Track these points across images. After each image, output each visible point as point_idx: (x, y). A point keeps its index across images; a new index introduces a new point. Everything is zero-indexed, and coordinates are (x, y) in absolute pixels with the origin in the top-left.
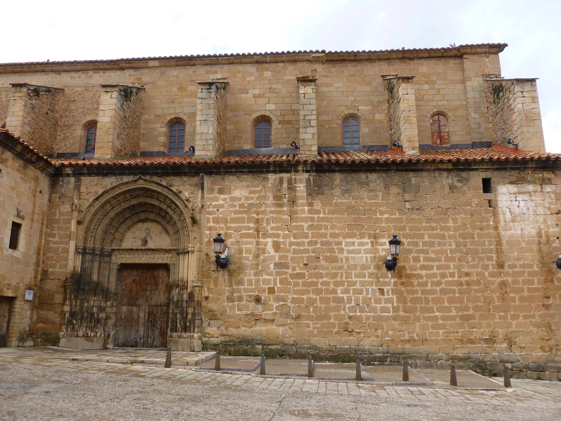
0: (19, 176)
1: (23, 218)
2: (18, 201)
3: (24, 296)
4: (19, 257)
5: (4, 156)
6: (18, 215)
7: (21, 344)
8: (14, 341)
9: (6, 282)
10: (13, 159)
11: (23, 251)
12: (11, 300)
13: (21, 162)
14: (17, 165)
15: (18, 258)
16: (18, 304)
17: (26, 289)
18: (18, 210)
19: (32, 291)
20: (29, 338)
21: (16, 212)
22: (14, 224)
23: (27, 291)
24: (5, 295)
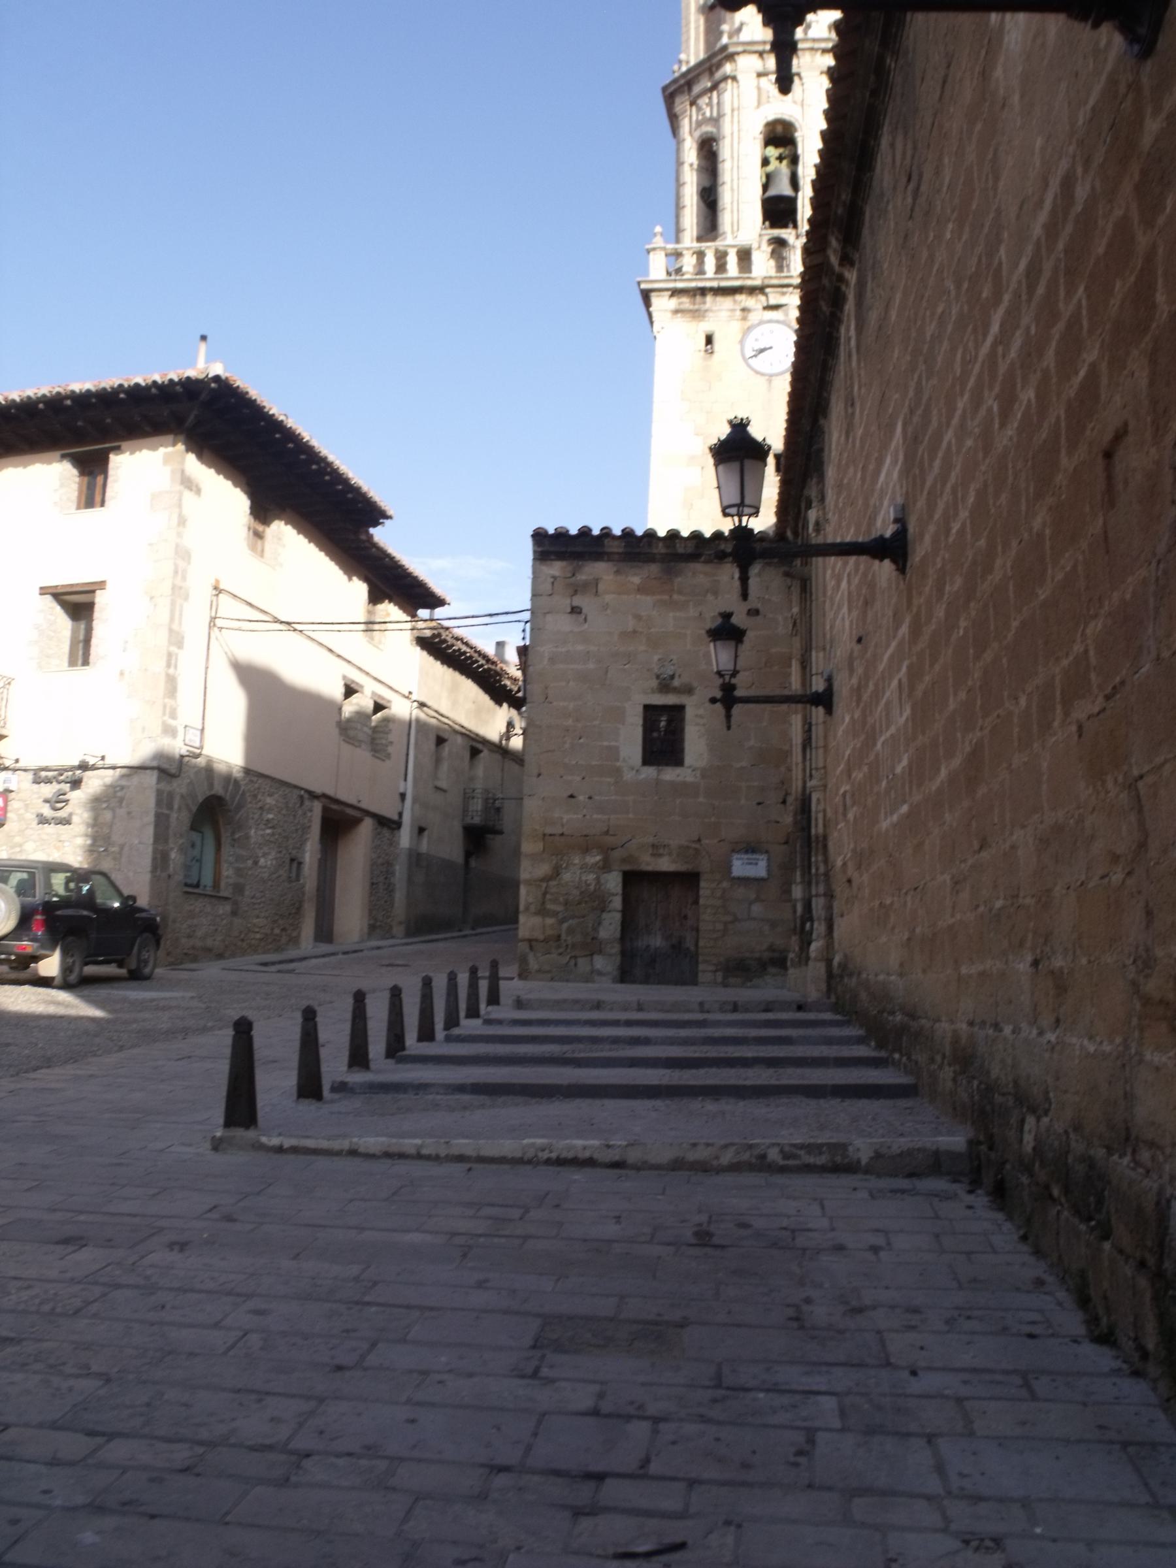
0: (646, 602)
1: (689, 690)
2: (656, 658)
3: (728, 867)
4: (689, 779)
5: (582, 577)
6: (665, 686)
7: (732, 980)
8: (706, 971)
9: (651, 840)
10: (617, 572)
11: (702, 763)
12: (690, 879)
13: (654, 569)
14: (636, 580)
15: (685, 784)
16: (705, 887)
17: (733, 851)
18: (658, 677)
19: (764, 857)
20: (772, 970)
21: (654, 683)
22: (648, 708)
23: (736, 856)
24: (650, 868)
